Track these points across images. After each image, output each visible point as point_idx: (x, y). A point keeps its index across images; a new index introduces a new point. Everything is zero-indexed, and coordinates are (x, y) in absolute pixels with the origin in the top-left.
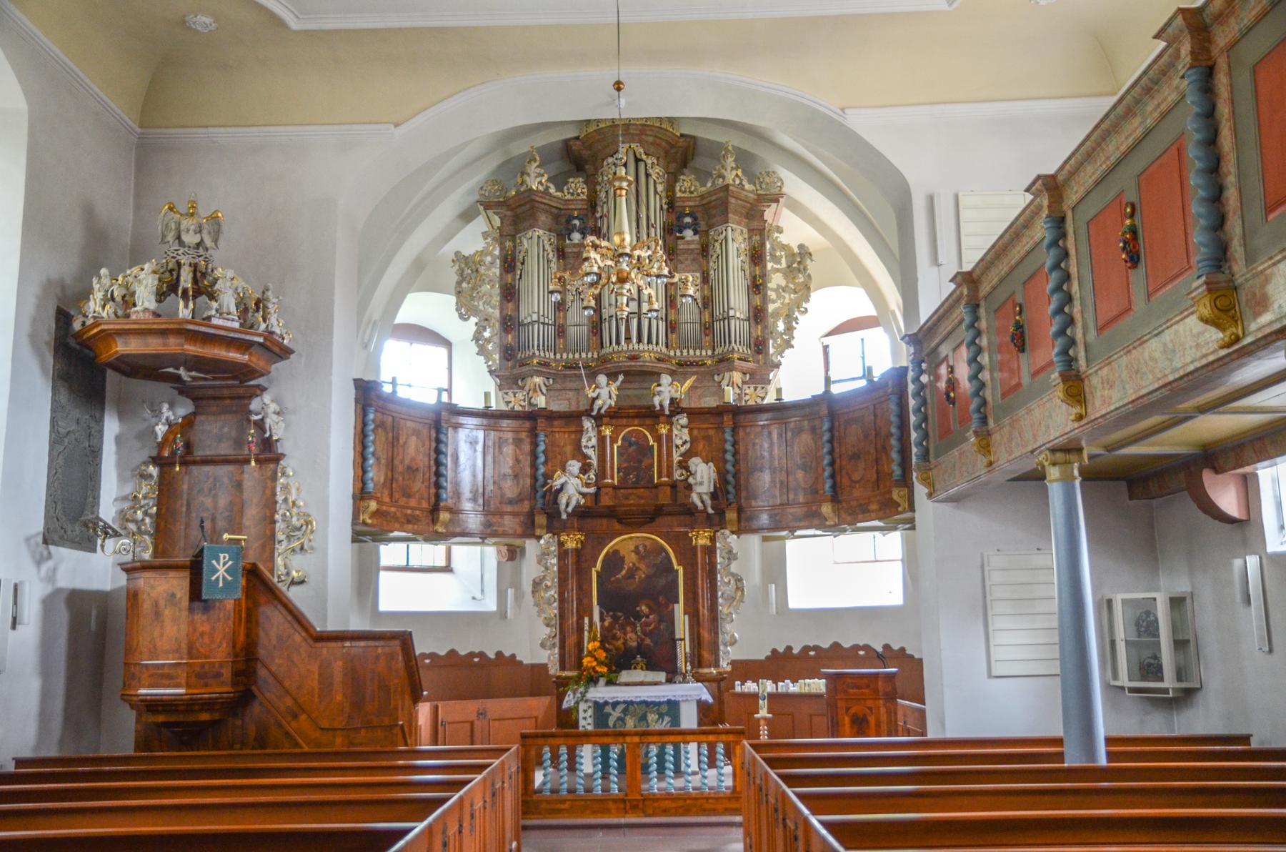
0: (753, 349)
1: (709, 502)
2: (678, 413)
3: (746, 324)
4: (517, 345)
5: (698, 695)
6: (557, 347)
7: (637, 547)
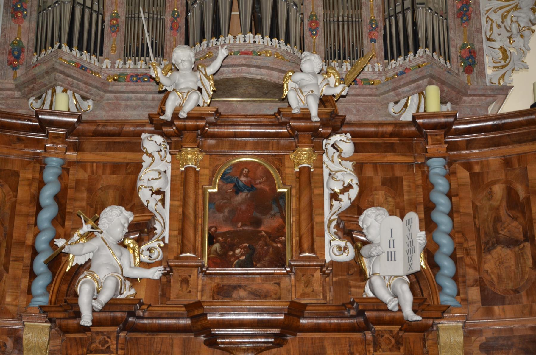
0: (455, 65)
1: (407, 298)
2: (336, 131)
4: (32, 43)
6: (106, 50)
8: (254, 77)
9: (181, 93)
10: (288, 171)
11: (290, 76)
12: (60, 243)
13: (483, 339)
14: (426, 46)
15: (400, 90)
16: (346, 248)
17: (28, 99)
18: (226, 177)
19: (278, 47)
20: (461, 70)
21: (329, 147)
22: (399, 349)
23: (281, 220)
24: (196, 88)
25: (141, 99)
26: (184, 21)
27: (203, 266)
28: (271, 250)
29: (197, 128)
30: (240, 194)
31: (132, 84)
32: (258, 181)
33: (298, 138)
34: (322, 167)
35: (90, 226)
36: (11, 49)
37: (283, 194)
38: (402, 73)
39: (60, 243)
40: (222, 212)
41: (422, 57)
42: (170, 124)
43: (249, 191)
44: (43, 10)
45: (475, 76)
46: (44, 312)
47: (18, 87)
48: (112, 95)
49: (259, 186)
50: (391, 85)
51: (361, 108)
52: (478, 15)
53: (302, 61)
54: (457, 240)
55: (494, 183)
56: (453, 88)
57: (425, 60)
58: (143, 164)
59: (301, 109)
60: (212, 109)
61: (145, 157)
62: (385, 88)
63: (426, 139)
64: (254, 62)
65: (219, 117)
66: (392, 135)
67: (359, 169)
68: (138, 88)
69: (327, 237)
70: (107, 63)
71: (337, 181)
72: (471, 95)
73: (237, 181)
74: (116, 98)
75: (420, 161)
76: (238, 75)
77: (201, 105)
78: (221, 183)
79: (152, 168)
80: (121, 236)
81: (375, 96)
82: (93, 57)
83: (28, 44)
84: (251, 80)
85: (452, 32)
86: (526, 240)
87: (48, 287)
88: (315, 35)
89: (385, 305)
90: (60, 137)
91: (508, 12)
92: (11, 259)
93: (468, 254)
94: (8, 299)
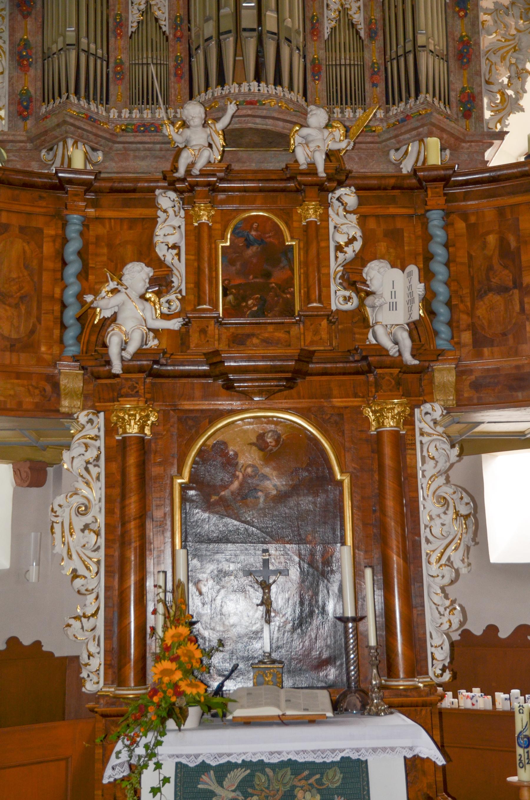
0: (455, 109)
1: (406, 343)
2: (341, 184)
3: (443, 66)
4: (39, 93)
5: (411, 749)
6: (112, 99)
7: (261, 437)
8: (259, 127)
9: (193, 150)
10: (295, 224)
11: (297, 130)
12: (89, 298)
13: (473, 377)
14: (427, 92)
15: (401, 137)
16: (350, 298)
17: (41, 151)
18: (237, 231)
19: (282, 95)
20: (461, 115)
21: (334, 200)
22: (399, 389)
23: (290, 272)
24: (207, 145)
25: (149, 150)
26: (187, 66)
27: (219, 317)
28: (281, 301)
29: (209, 184)
30: (251, 248)
31: (140, 134)
32: (267, 235)
33: (304, 192)
34: (328, 221)
35: (116, 283)
36: (20, 99)
37: (292, 246)
38: (403, 120)
39: (89, 298)
40: (234, 265)
41: (423, 103)
42: (183, 180)
43: (260, 244)
44: (49, 57)
45: (473, 120)
46: (76, 361)
47: (30, 140)
48: (120, 146)
49: (268, 240)
50: (392, 133)
51: (363, 156)
52: (478, 57)
53: (309, 115)
54: (452, 288)
55: (488, 233)
56: (452, 135)
57: (426, 107)
58: (158, 219)
59: (308, 164)
60: (223, 166)
61: (160, 213)
62: (387, 136)
63: (426, 191)
64: (259, 113)
65: (229, 173)
66: (394, 188)
67: (362, 221)
68: (146, 139)
69: (333, 288)
70: (113, 113)
71: (341, 233)
72: (468, 142)
73: (248, 235)
74: (125, 149)
75: (420, 212)
76: (244, 126)
77: (212, 161)
78: (233, 238)
79: (167, 223)
80: (143, 291)
81: (377, 143)
82: (100, 107)
83: (36, 93)
84: (257, 130)
85: (452, 75)
86: (515, 287)
87: (78, 338)
88: (318, 80)
89: (387, 351)
90: (79, 195)
91: (507, 52)
92: (43, 312)
93: (462, 301)
94: (43, 349)
